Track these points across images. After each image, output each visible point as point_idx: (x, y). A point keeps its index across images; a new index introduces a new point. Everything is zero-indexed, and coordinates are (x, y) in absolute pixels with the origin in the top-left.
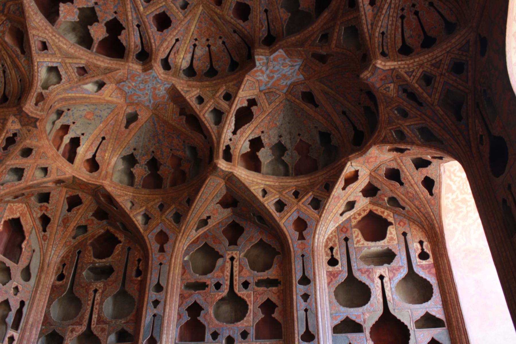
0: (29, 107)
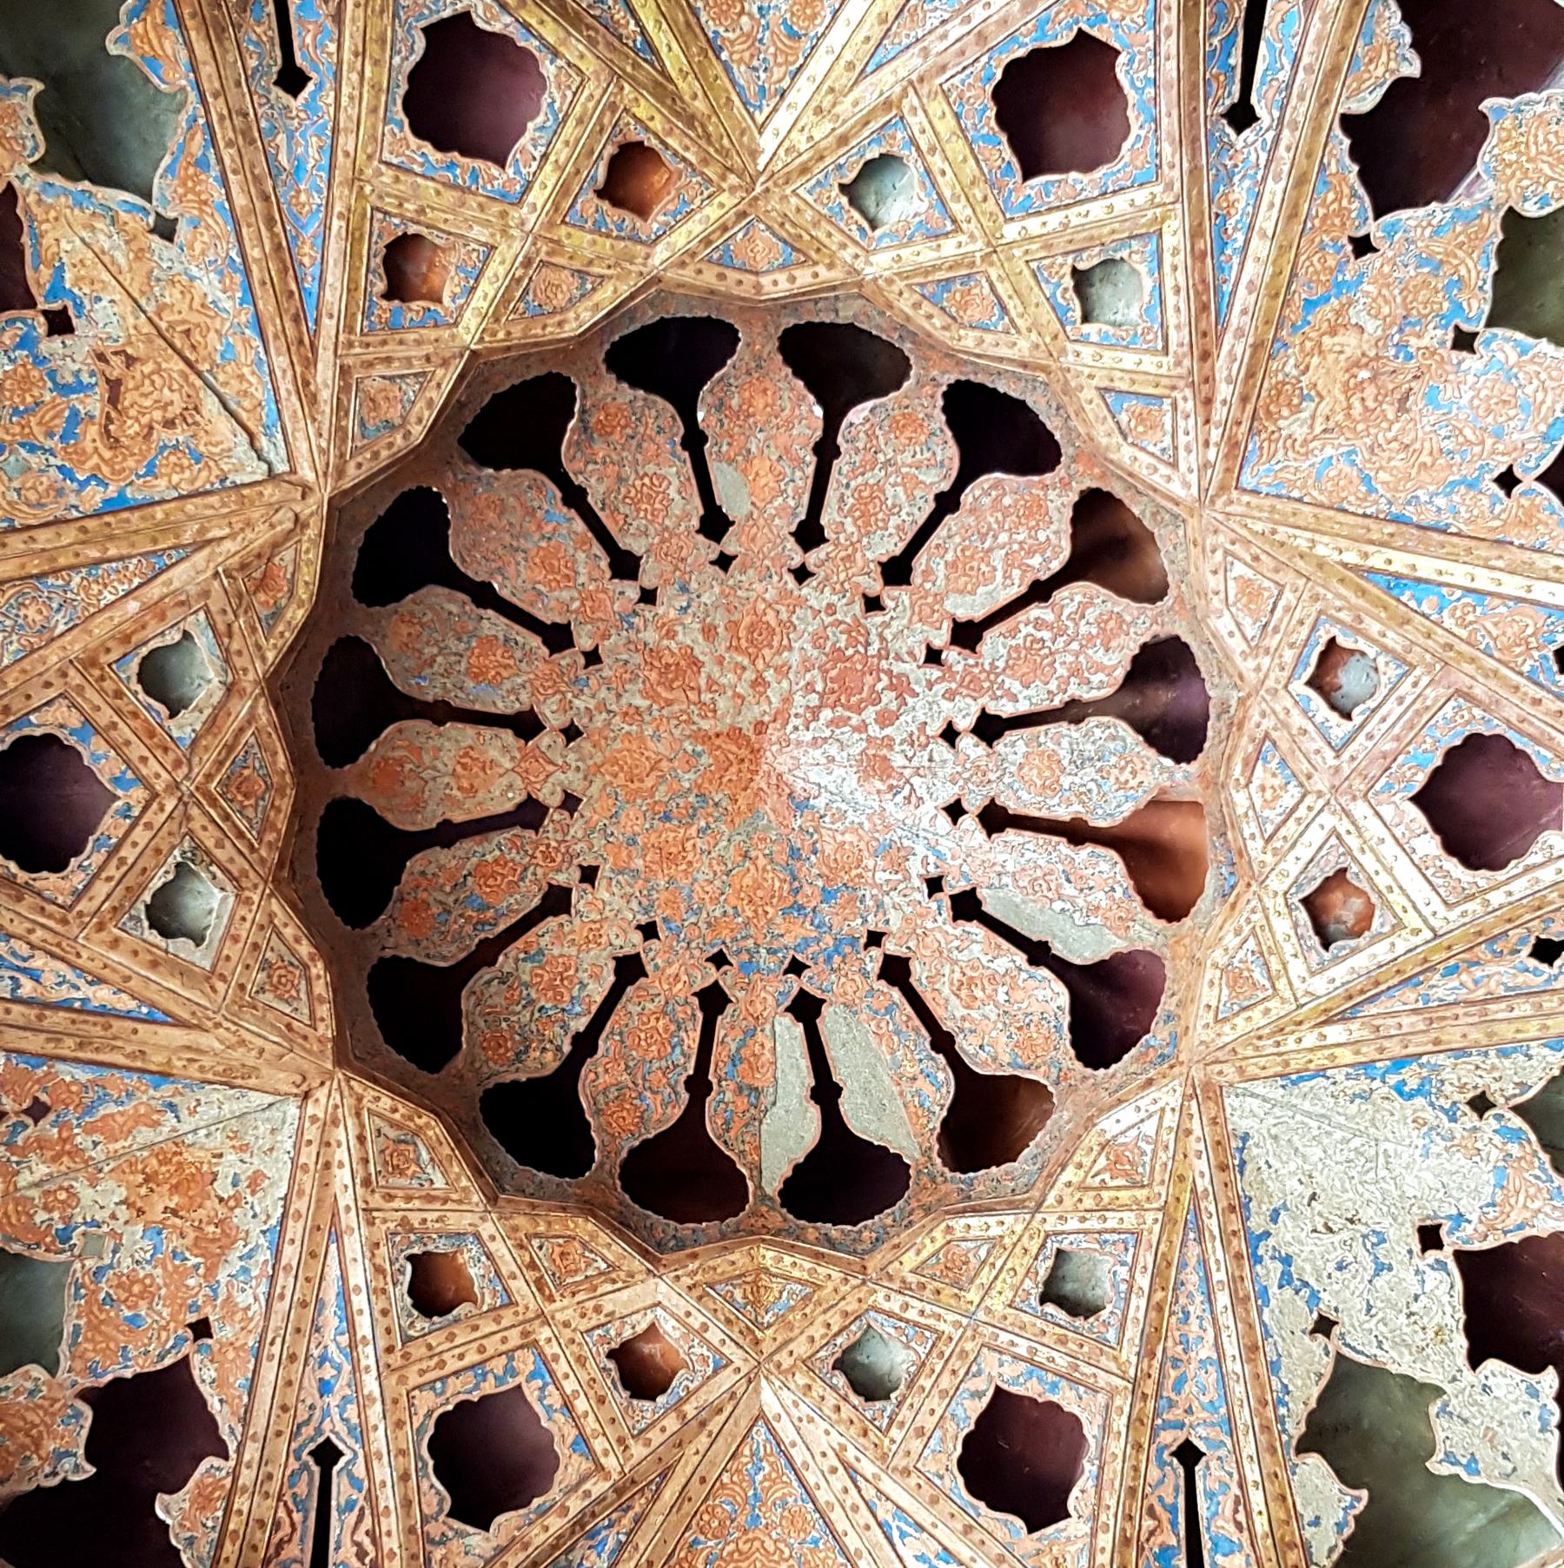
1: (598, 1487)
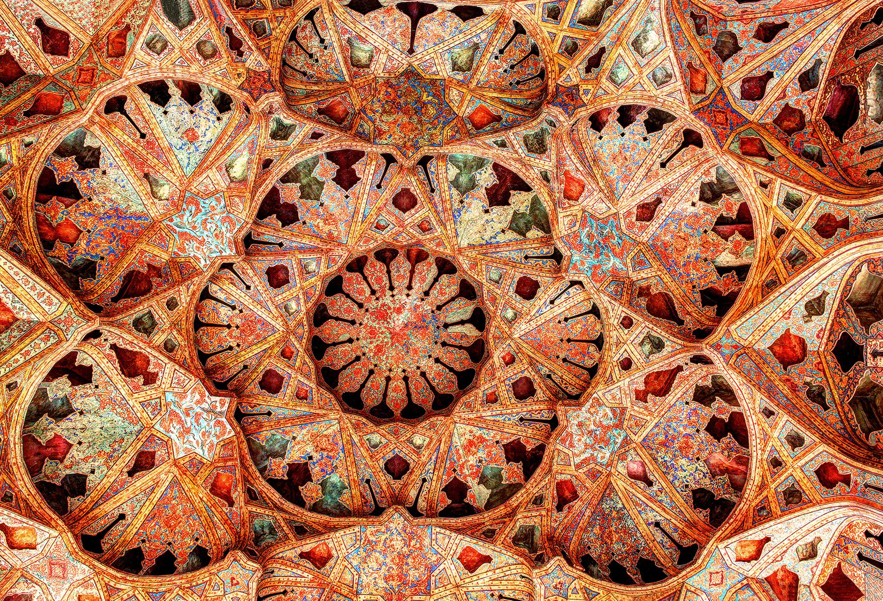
0: (276, 99)
1: (530, 369)
